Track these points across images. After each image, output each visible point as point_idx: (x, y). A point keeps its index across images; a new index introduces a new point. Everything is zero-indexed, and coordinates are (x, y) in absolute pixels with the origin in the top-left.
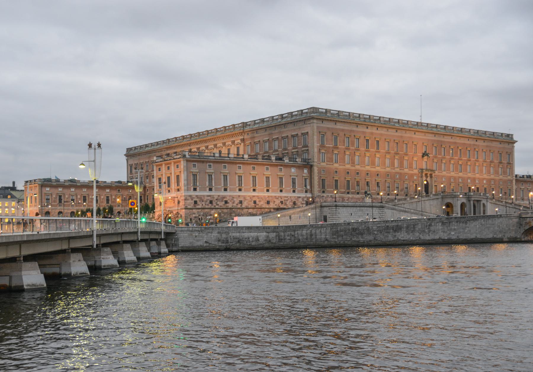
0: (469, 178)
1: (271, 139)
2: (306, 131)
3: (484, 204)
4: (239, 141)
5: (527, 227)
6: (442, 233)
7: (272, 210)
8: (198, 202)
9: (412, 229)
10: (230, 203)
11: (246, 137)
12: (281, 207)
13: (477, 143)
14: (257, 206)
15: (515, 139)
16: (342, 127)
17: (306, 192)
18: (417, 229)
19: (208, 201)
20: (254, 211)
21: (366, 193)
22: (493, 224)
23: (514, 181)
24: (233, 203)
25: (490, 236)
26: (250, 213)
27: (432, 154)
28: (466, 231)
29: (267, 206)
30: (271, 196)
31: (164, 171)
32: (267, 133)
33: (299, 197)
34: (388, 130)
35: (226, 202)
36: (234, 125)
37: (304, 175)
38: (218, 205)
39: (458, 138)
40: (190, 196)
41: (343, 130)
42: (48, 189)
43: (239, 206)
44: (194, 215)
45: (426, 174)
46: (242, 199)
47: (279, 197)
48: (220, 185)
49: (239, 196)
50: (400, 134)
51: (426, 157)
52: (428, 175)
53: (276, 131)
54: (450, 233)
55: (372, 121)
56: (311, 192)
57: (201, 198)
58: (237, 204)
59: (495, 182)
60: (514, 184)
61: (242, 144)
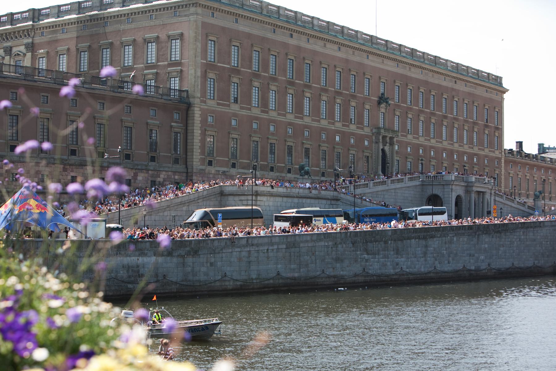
0: (445, 149)
1: (95, 46)
2: (179, 31)
4: (22, 48)
11: (37, 40)
13: (456, 87)
15: (505, 85)
16: (247, 30)
17: (176, 161)
21: (302, 168)
22: (535, 240)
23: (503, 161)
25: (530, 263)
27: (393, 99)
36: (12, 14)
39: (431, 74)
45: (384, 137)
51: (383, 105)
52: (388, 139)
59: (478, 160)
60: (503, 165)
61: (29, 55)
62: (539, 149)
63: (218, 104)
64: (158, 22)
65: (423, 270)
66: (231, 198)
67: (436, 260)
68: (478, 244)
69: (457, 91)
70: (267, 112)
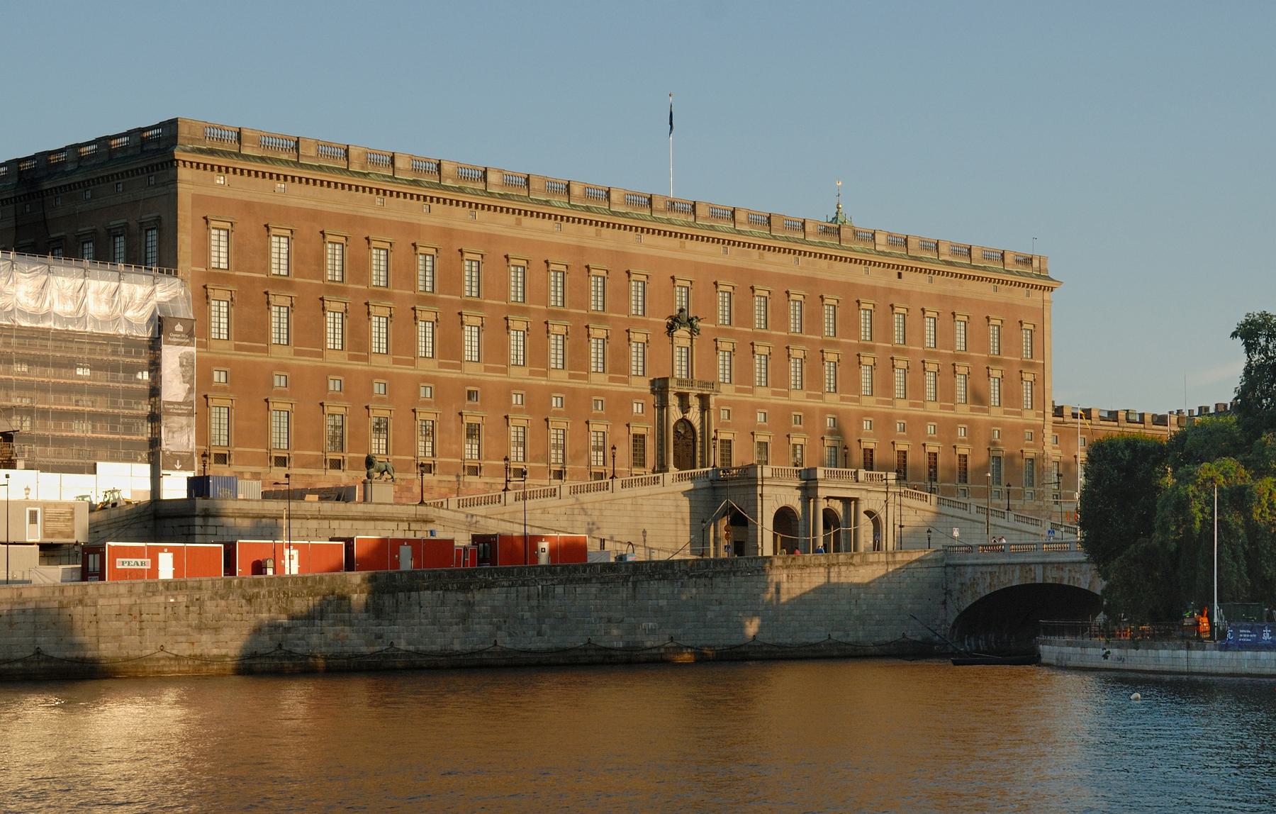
0: (867, 414)
5: (968, 601)
16: (309, 204)
28: (710, 615)
41: (314, 215)
45: (683, 397)
50: (573, 241)
51: (682, 333)
55: (448, 183)
65: (457, 646)
66: (168, 523)
67: (499, 628)
68: (634, 598)
69: (906, 295)
70: (366, 359)
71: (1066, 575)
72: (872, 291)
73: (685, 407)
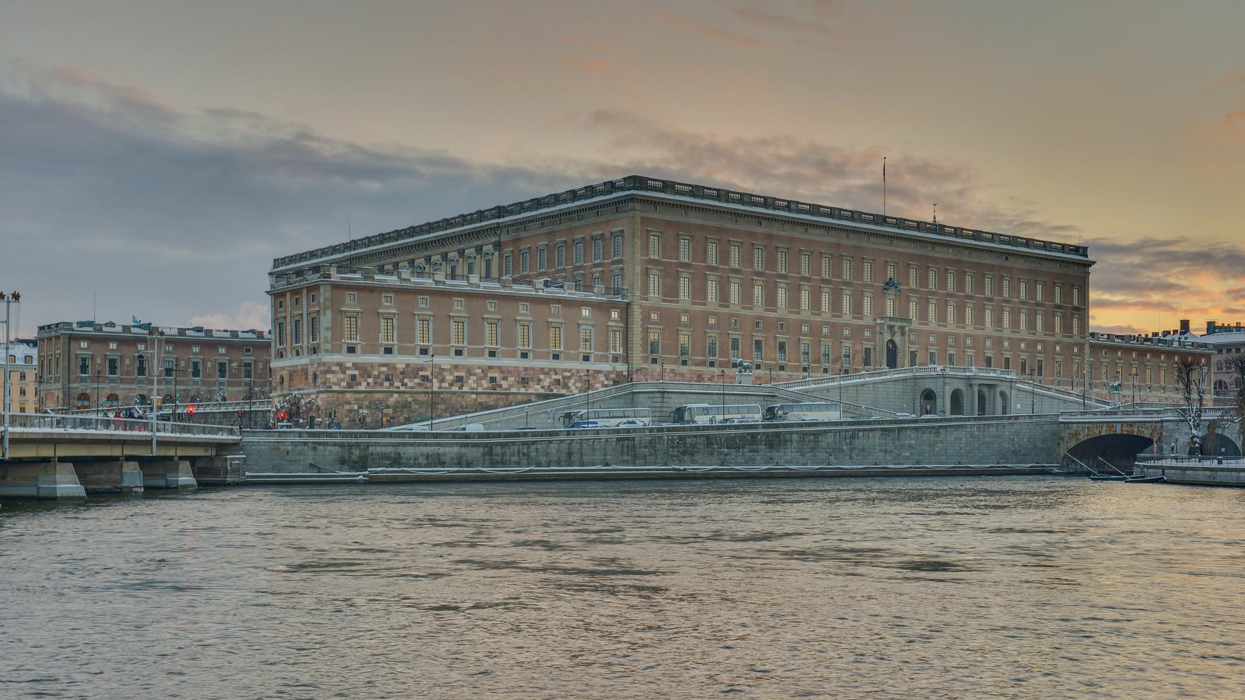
0: (988, 337)
3: (1003, 394)
5: (1072, 444)
6: (881, 455)
7: (533, 398)
8: (359, 379)
9: (812, 445)
10: (435, 381)
11: (504, 238)
12: (555, 391)
14: (498, 390)
16: (699, 222)
17: (616, 359)
18: (824, 444)
19: (383, 377)
20: (491, 400)
22: (1000, 437)
23: (1087, 347)
24: (442, 380)
26: (481, 404)
29: (523, 390)
30: (533, 369)
31: (289, 309)
32: (545, 230)
33: (599, 372)
34: (806, 230)
35: (425, 378)
37: (611, 324)
38: (404, 385)
39: (966, 252)
40: (340, 365)
42: (84, 345)
43: (455, 389)
44: (347, 407)
45: (891, 327)
46: (463, 374)
47: (550, 369)
48: (413, 340)
49: (456, 367)
51: (892, 291)
53: (563, 226)
54: (899, 455)
56: (627, 360)
57: (365, 371)
58: (451, 385)
59: (1044, 347)
62: (1208, 329)
63: (664, 301)
64: (603, 219)
71: (1136, 430)
72: (992, 268)
73: (893, 334)
